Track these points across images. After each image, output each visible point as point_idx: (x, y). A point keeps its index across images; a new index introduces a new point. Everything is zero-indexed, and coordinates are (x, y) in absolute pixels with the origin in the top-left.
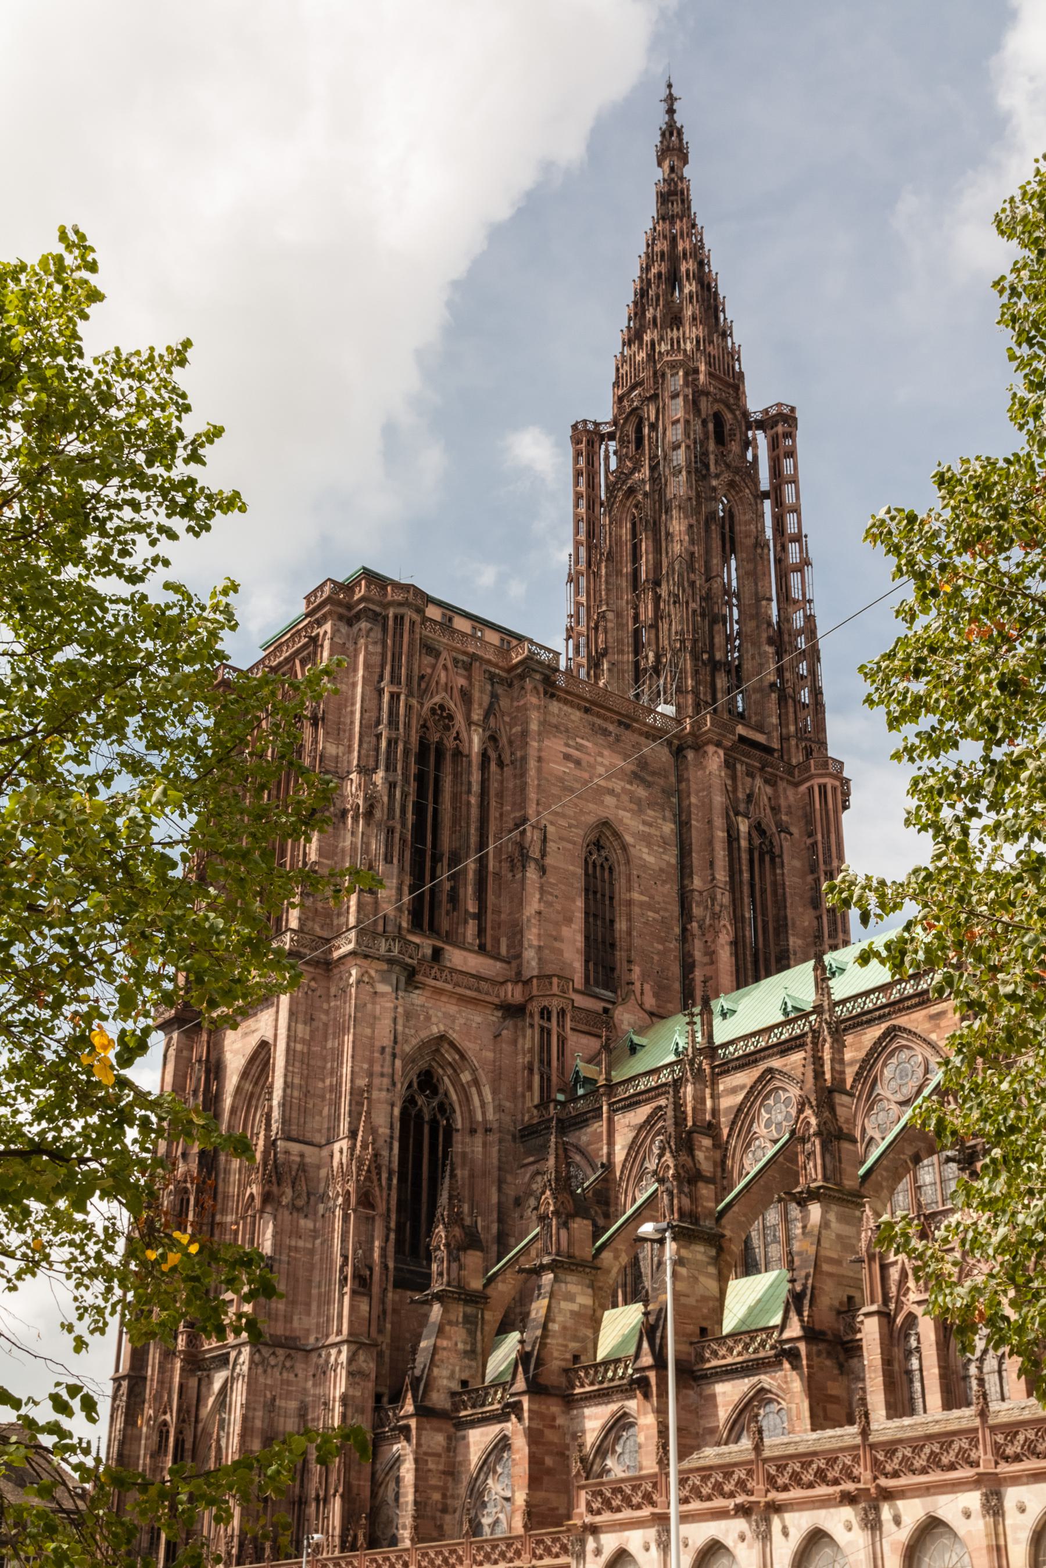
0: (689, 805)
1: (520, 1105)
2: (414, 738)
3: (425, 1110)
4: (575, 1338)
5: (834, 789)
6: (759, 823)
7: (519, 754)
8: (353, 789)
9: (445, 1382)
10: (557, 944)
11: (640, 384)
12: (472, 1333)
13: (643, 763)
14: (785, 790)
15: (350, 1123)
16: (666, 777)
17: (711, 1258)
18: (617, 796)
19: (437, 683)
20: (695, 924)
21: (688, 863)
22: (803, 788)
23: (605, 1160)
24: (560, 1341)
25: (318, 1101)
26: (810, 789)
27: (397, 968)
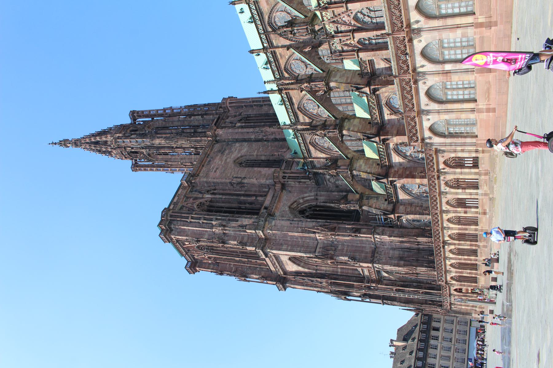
1: (310, 186)
2: (205, 213)
4: (372, 165)
5: (230, 100)
6: (239, 120)
7: (212, 184)
8: (218, 230)
9: (385, 206)
10: (267, 175)
12: (372, 198)
17: (348, 122)
18: (227, 158)
19: (191, 206)
20: (264, 138)
21: (247, 140)
22: (230, 109)
23: (325, 160)
24: (373, 169)
25: (305, 243)
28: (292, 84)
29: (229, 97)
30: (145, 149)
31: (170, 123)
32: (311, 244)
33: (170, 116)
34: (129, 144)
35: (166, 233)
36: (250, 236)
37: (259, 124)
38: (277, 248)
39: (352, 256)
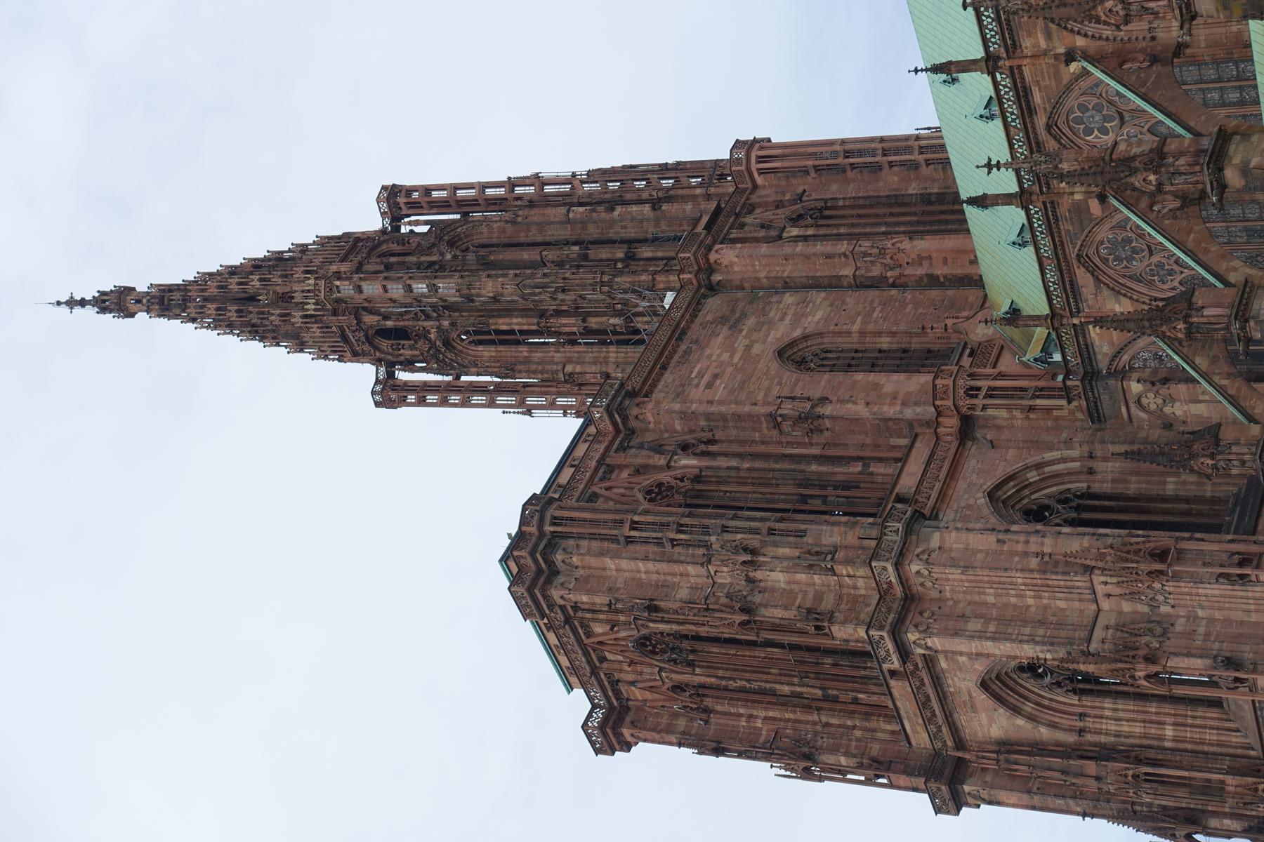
0: (767, 278)
2: (681, 510)
5: (761, 148)
6: (791, 219)
7: (703, 423)
10: (901, 396)
11: (341, 328)
13: (723, 320)
14: (760, 197)
18: (753, 342)
20: (889, 274)
22: (759, 180)
26: (762, 172)
27: (916, 527)
29: (755, 141)
31: (534, 228)
33: (531, 203)
36: (845, 591)
38: (946, 629)
39: (1228, 655)
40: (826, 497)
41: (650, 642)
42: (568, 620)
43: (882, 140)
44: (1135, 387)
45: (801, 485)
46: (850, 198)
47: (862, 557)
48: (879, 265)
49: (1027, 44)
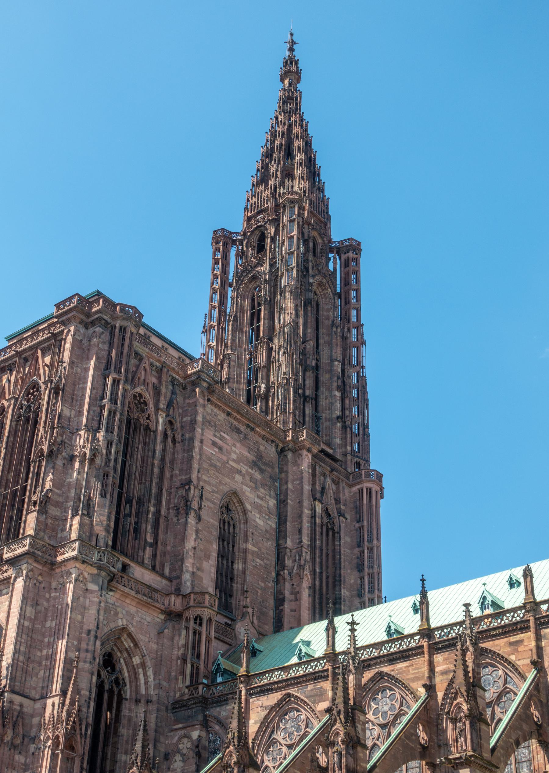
0: (287, 489)
1: (173, 685)
3: (106, 682)
5: (376, 492)
6: (327, 508)
7: (187, 436)
10: (199, 573)
13: (260, 457)
14: (343, 488)
15: (62, 684)
16: (273, 468)
18: (243, 476)
19: (139, 378)
20: (286, 571)
22: (355, 489)
25: (36, 666)
26: (361, 491)
28: (466, 673)
29: (382, 489)
30: (270, 271)
31: (328, 339)
32: (32, 682)
33: (344, 338)
34: (284, 234)
35: (83, 312)
37: (318, 560)
40: (130, 517)
41: (36, 391)
42: (54, 335)
43: (379, 573)
44: (195, 734)
45: (140, 500)
46: (340, 550)
47: (84, 535)
48: (293, 565)
49: (439, 658)
